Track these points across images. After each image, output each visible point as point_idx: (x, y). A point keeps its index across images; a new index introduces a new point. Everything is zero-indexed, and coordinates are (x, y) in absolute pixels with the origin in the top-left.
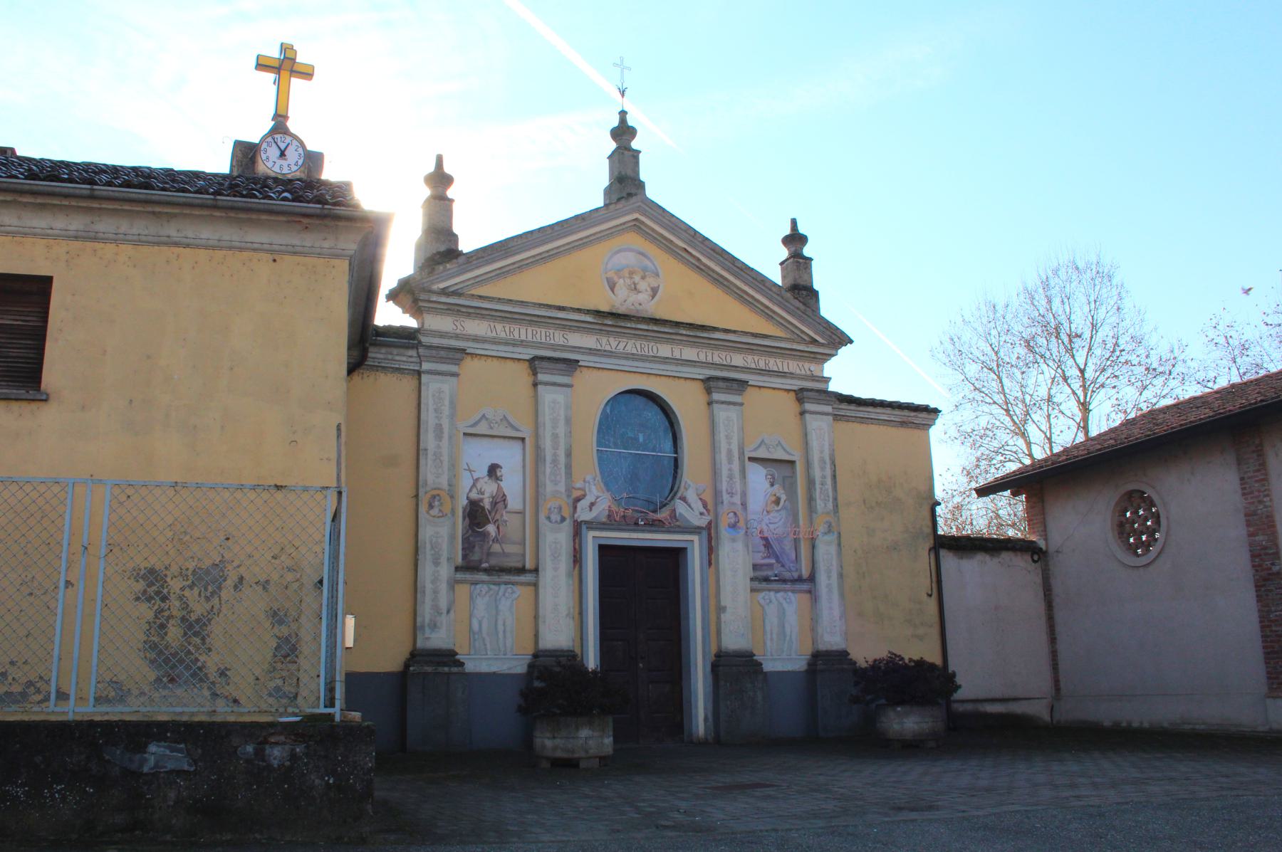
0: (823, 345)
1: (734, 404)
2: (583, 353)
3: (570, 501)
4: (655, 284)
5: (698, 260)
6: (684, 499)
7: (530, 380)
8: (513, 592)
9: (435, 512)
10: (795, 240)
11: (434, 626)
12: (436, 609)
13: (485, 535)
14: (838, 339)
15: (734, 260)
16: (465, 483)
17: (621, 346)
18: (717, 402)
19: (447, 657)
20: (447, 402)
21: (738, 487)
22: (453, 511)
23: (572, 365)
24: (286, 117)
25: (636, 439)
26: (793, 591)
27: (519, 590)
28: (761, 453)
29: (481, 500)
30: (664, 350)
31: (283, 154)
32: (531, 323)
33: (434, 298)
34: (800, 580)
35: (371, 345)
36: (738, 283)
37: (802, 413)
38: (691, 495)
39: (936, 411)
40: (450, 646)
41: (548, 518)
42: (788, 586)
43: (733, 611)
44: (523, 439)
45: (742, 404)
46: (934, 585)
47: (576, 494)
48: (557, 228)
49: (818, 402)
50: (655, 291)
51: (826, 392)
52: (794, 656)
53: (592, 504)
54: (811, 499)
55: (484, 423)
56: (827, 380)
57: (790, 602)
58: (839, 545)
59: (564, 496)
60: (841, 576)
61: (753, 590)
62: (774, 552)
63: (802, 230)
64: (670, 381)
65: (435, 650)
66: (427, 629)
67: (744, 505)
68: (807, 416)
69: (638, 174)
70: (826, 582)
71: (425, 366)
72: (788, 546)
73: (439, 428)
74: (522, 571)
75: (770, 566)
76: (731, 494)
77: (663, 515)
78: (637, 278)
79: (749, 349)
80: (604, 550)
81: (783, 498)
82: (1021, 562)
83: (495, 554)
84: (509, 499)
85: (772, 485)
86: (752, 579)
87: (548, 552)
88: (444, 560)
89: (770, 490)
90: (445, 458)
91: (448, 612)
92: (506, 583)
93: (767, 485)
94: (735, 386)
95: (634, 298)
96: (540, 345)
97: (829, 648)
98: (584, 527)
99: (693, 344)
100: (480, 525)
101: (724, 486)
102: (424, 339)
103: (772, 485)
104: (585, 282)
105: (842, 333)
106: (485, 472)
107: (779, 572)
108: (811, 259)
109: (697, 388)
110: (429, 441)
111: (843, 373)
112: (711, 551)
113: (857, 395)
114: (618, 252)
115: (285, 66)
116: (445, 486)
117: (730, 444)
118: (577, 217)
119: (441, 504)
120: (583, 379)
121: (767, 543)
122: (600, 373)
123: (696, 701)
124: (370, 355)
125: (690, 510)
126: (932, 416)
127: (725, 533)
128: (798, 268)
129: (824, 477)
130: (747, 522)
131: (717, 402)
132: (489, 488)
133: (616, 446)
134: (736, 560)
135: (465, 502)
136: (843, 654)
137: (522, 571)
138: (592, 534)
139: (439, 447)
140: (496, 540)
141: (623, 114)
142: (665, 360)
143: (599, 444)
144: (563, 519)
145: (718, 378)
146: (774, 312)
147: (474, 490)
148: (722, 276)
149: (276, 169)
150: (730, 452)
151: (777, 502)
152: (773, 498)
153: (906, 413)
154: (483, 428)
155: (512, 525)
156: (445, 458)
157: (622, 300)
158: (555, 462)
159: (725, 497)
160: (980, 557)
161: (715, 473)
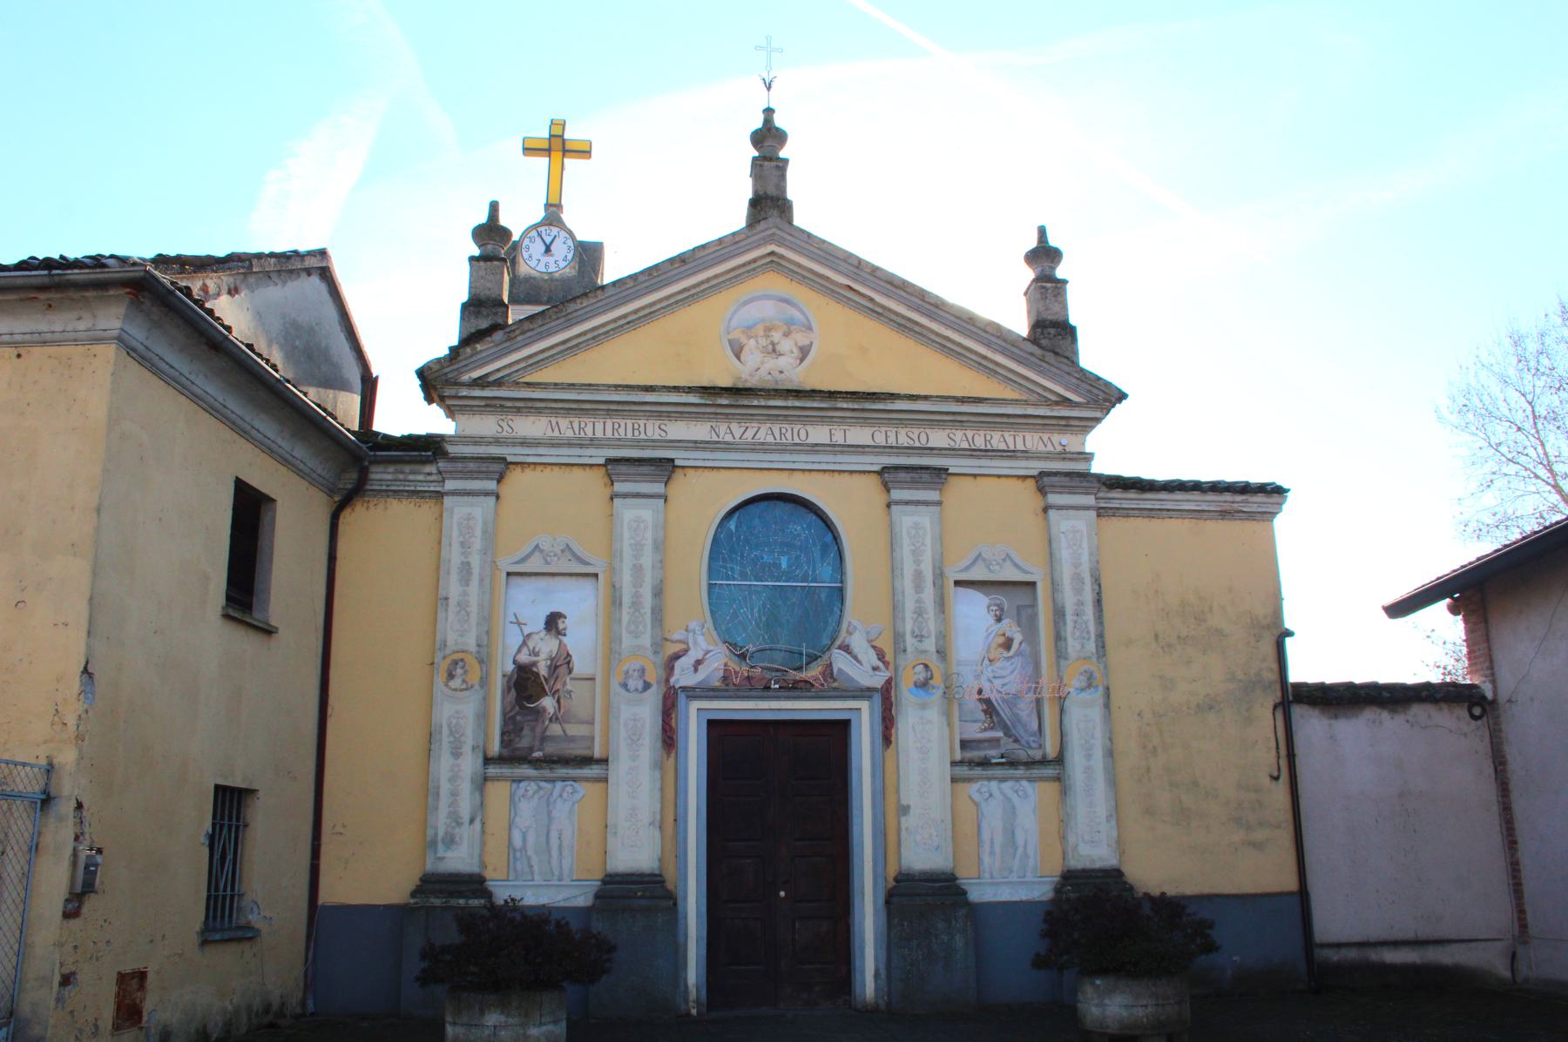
1: (926, 503)
2: (686, 449)
3: (660, 660)
4: (804, 341)
5: (871, 300)
6: (846, 648)
7: (607, 492)
8: (575, 791)
9: (456, 683)
10: (1044, 255)
11: (450, 841)
12: (456, 819)
13: (539, 713)
14: (1106, 397)
15: (922, 295)
16: (514, 640)
17: (749, 434)
18: (897, 503)
19: (474, 884)
20: (478, 532)
21: (932, 625)
22: (484, 682)
23: (665, 468)
24: (559, 206)
26: (1030, 780)
27: (582, 788)
28: (978, 574)
29: (534, 664)
31: (548, 250)
32: (609, 413)
33: (464, 392)
34: (1044, 762)
35: (371, 463)
36: (934, 326)
37: (1045, 510)
38: (858, 643)
39: (1277, 491)
40: (475, 869)
41: (625, 686)
42: (1020, 772)
43: (917, 810)
44: (596, 575)
45: (939, 503)
46: (1284, 763)
47: (673, 649)
48: (641, 278)
49: (1071, 491)
50: (804, 352)
51: (1085, 476)
52: (1029, 877)
53: (698, 663)
54: (1059, 638)
55: (537, 557)
56: (1088, 457)
57: (1026, 796)
58: (1107, 705)
59: (649, 653)
60: (1110, 753)
61: (954, 780)
62: (1002, 721)
63: (1053, 242)
64: (827, 476)
65: (451, 875)
66: (440, 846)
67: (942, 653)
68: (1051, 513)
69: (783, 190)
70: (1085, 764)
71: (450, 485)
72: (1025, 710)
73: (466, 568)
74: (587, 761)
75: (995, 742)
76: (920, 638)
77: (813, 672)
80: (718, 729)
81: (1018, 638)
83: (553, 738)
84: (575, 659)
85: (999, 620)
86: (954, 763)
87: (623, 733)
88: (467, 748)
90: (474, 609)
91: (472, 821)
92: (564, 779)
93: (992, 620)
94: (926, 476)
95: (772, 363)
96: (620, 443)
97: (1088, 865)
98: (682, 697)
99: (865, 422)
100: (531, 699)
102: (450, 449)
103: (999, 620)
104: (692, 346)
105: (1108, 384)
106: (542, 625)
107: (1001, 749)
108: (1064, 282)
109: (873, 483)
110: (453, 589)
111: (1112, 448)
112: (888, 722)
113: (1147, 474)
114: (746, 303)
115: (557, 147)
116: (473, 647)
117: (918, 562)
118: (671, 261)
119: (466, 672)
120: (685, 488)
121: (989, 708)
122: (707, 473)
123: (862, 949)
124: (373, 476)
126: (1275, 498)
127: (907, 696)
128: (1044, 297)
129: (1080, 603)
130: (947, 677)
131: (897, 503)
132: (547, 647)
133: (744, 576)
134: (926, 736)
135: (510, 667)
136: (1115, 874)
137: (587, 761)
138: (695, 705)
139: (465, 594)
141: (769, 112)
142: (815, 448)
143: (712, 572)
144: (647, 686)
145: (897, 468)
147: (525, 650)
148: (910, 320)
149: (541, 268)
150: (918, 575)
151: (1007, 644)
152: (1001, 640)
153: (1228, 497)
154: (535, 564)
155: (578, 696)
156: (474, 609)
157: (754, 368)
158: (636, 604)
159: (910, 642)
160: (1369, 713)
161: (896, 608)
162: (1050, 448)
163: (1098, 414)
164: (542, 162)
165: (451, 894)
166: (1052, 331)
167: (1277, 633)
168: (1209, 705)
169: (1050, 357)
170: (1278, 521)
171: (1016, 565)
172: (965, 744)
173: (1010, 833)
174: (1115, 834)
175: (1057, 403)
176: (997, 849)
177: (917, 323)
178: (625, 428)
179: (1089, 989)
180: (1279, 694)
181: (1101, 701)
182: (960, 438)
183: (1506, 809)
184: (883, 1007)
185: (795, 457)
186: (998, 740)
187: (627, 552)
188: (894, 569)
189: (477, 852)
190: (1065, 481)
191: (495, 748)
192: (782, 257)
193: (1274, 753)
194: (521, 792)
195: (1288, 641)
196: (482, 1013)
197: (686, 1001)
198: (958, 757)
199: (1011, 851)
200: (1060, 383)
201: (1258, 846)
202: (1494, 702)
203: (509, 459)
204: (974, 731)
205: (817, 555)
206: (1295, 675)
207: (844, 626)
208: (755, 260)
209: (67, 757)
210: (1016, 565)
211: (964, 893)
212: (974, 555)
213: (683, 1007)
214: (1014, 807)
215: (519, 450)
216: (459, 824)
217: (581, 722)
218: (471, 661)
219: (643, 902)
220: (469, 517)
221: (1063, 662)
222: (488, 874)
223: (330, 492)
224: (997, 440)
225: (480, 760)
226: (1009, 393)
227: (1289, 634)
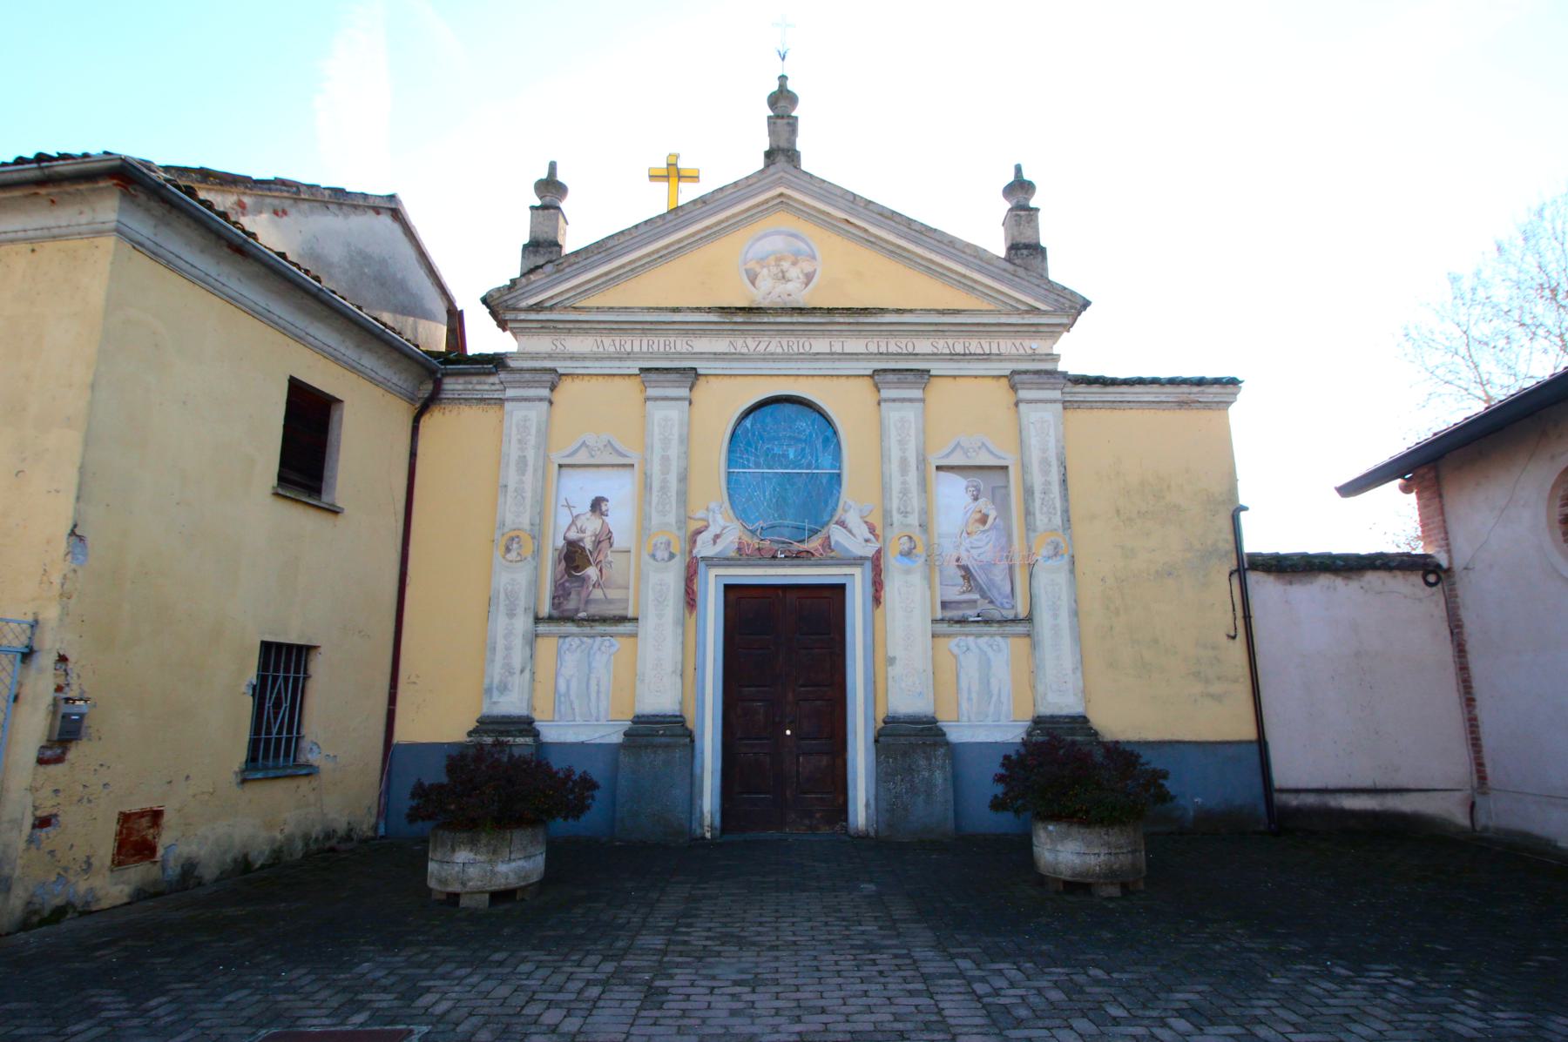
0: (1045, 313)
1: (911, 400)
4: (808, 268)
5: (866, 231)
6: (842, 524)
8: (612, 645)
9: (513, 556)
10: (1020, 188)
11: (504, 688)
13: (583, 580)
15: (909, 222)
16: (564, 520)
18: (886, 400)
20: (533, 431)
21: (915, 502)
22: (537, 553)
23: (691, 376)
25: (785, 456)
26: (1003, 636)
29: (581, 540)
30: (820, 345)
33: (522, 316)
34: (1015, 621)
35: (446, 375)
36: (919, 251)
38: (853, 519)
39: (1234, 382)
41: (653, 556)
42: (994, 629)
43: (899, 663)
46: (1240, 623)
47: (694, 526)
49: (1040, 386)
50: (809, 277)
51: (1052, 373)
53: (717, 537)
54: (1028, 513)
58: (1072, 571)
60: (1075, 613)
61: (933, 636)
63: (1026, 176)
64: (827, 380)
66: (495, 693)
68: (1022, 406)
69: (794, 143)
70: (1053, 622)
71: (510, 393)
72: (999, 575)
73: (523, 461)
74: (622, 619)
76: (905, 514)
77: (814, 544)
78: (785, 265)
79: (938, 330)
80: (733, 592)
81: (992, 514)
82: (1408, 586)
83: (596, 601)
84: (614, 535)
85: (976, 499)
86: (934, 621)
87: (651, 596)
88: (520, 611)
89: (973, 505)
90: (528, 495)
91: (522, 671)
93: (969, 499)
94: (910, 377)
95: (782, 288)
96: (652, 355)
98: (702, 566)
100: (577, 568)
101: (895, 504)
102: (512, 364)
103: (976, 499)
106: (588, 508)
108: (1037, 210)
109: (867, 384)
110: (512, 479)
112: (877, 585)
113: (1109, 373)
114: (759, 239)
116: (526, 526)
117: (904, 450)
121: (967, 574)
122: (727, 381)
124: (446, 387)
125: (851, 537)
126: (1230, 389)
128: (1018, 224)
129: (1048, 483)
130: (929, 546)
131: (886, 400)
132: (592, 525)
133: (758, 465)
135: (561, 543)
136: (1080, 722)
137: (622, 619)
138: (713, 572)
139: (521, 482)
140: (597, 585)
141: (783, 78)
142: (817, 357)
143: (731, 462)
144: (672, 556)
146: (975, 281)
147: (574, 529)
148: (899, 247)
150: (904, 462)
151: (983, 520)
152: (978, 516)
153: (1185, 388)
154: (582, 458)
156: (528, 495)
157: (766, 292)
158: (664, 488)
159: (896, 517)
160: (1324, 580)
161: (885, 489)
162: (1022, 351)
163: (1065, 321)
164: (662, 187)
165: (502, 733)
166: (1025, 252)
167: (1232, 508)
168: (1168, 572)
169: (1021, 272)
170: (1232, 409)
171: (991, 453)
172: (945, 605)
173: (986, 682)
174: (1080, 684)
175: (1027, 312)
176: (974, 696)
177: (904, 249)
178: (658, 343)
179: (1042, 834)
180: (1235, 562)
181: (1067, 567)
182: (942, 345)
183: (1463, 668)
184: (872, 834)
185: (799, 365)
186: (975, 601)
187: (657, 445)
188: (883, 456)
189: (526, 696)
190: (1035, 378)
191: (545, 609)
192: (789, 197)
193: (1230, 614)
194: (566, 646)
195: (1243, 514)
196: (453, 850)
197: (702, 826)
198: (939, 615)
199: (987, 700)
200: (1029, 295)
201: (1218, 698)
202: (1449, 571)
203: (560, 371)
204: (954, 594)
205: (819, 445)
206: (1250, 547)
207: (841, 504)
208: (766, 201)
209: (51, 614)
210: (991, 453)
211: (944, 734)
212: (952, 445)
213: (699, 831)
214: (989, 661)
215: (569, 363)
216: (512, 674)
217: (619, 587)
218: (526, 538)
219: (663, 740)
220: (526, 419)
221: (1032, 535)
222: (536, 716)
223: (411, 400)
224: (974, 346)
225: (531, 619)
226: (984, 306)
227: (1246, 509)
